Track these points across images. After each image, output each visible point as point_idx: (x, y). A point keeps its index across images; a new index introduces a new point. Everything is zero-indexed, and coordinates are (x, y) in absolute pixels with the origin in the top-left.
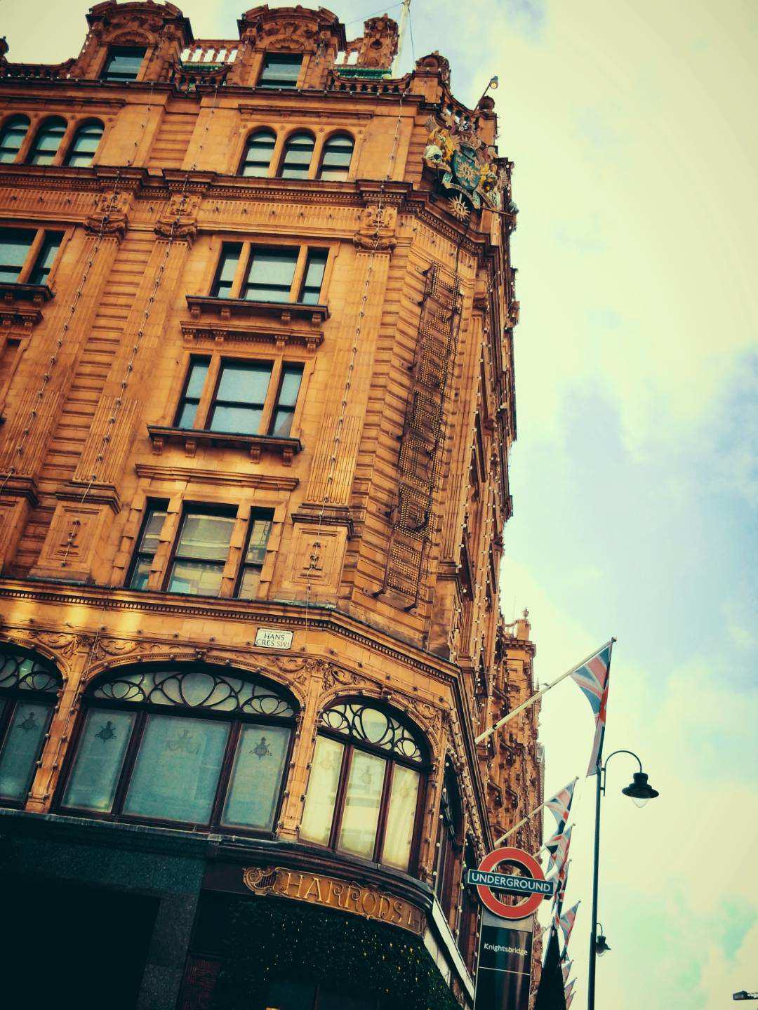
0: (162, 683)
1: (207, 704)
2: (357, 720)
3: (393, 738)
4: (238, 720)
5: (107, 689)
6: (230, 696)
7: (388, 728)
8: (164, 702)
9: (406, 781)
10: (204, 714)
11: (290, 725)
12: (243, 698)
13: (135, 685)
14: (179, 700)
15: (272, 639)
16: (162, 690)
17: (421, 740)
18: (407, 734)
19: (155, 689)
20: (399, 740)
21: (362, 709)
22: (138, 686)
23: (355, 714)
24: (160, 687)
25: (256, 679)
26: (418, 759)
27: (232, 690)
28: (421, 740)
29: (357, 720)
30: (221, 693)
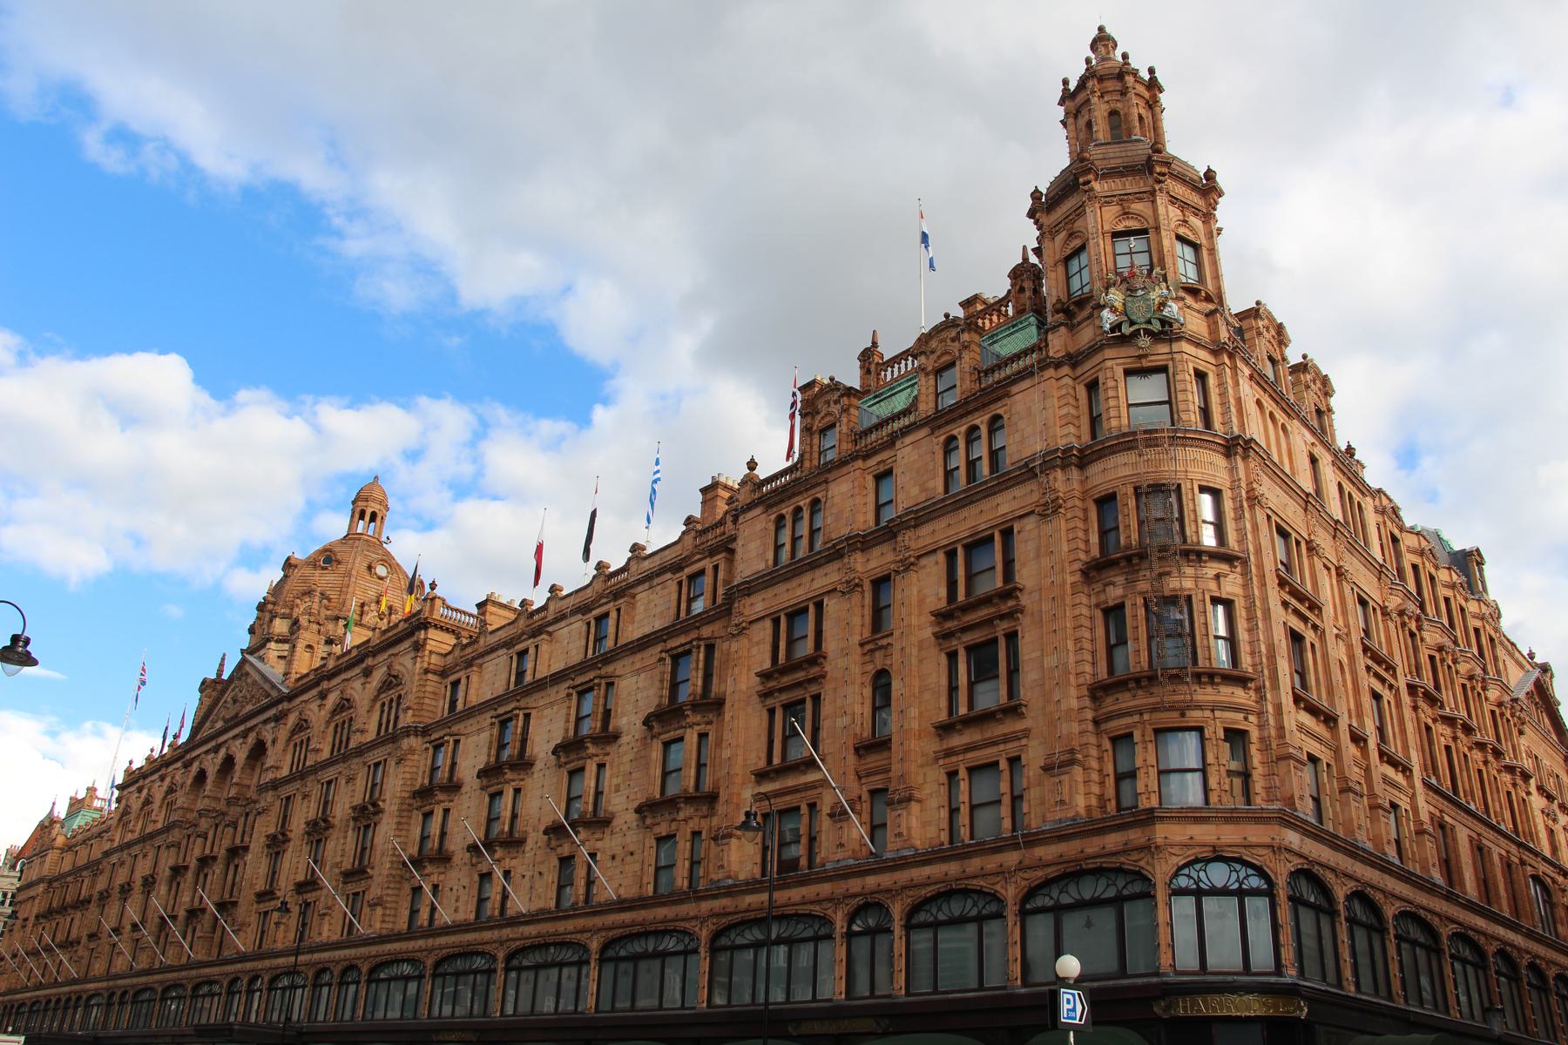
1: (1096, 895)
2: (1202, 874)
4: (1118, 901)
8: (1072, 901)
9: (1258, 907)
10: (1096, 903)
11: (1148, 896)
14: (1078, 897)
16: (1067, 892)
17: (1261, 872)
18: (1250, 871)
19: (1061, 892)
20: (1245, 878)
25: (1119, 871)
28: (1261, 872)
29: (1202, 874)
30: (1103, 882)
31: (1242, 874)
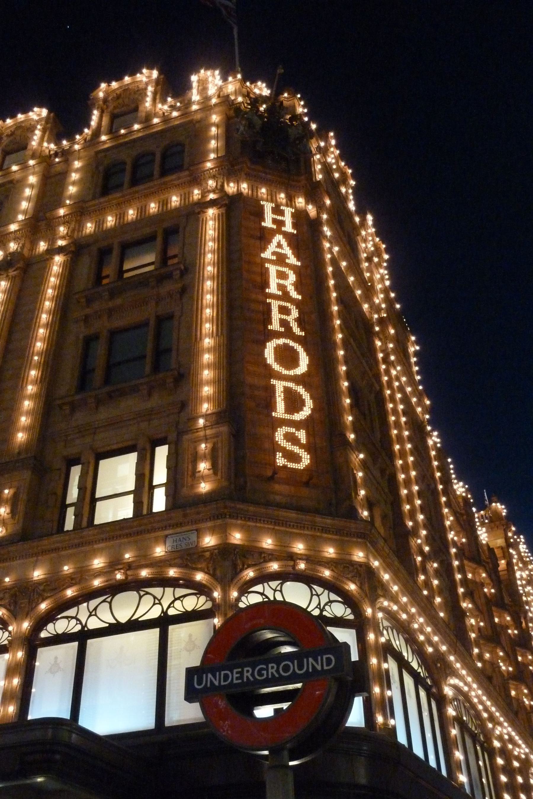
0: (95, 609)
3: (319, 604)
5: (50, 627)
6: (154, 604)
7: (312, 595)
12: (165, 604)
13: (72, 618)
15: (180, 543)
16: (96, 615)
18: (333, 597)
21: (282, 584)
22: (75, 618)
23: (275, 590)
24: (93, 613)
26: (351, 617)
27: (155, 598)
31: (324, 599)
